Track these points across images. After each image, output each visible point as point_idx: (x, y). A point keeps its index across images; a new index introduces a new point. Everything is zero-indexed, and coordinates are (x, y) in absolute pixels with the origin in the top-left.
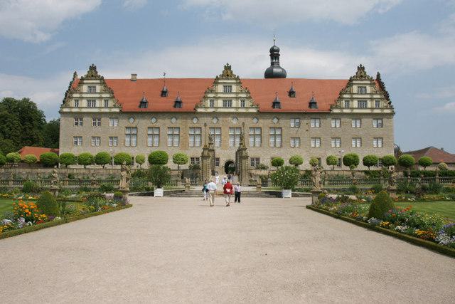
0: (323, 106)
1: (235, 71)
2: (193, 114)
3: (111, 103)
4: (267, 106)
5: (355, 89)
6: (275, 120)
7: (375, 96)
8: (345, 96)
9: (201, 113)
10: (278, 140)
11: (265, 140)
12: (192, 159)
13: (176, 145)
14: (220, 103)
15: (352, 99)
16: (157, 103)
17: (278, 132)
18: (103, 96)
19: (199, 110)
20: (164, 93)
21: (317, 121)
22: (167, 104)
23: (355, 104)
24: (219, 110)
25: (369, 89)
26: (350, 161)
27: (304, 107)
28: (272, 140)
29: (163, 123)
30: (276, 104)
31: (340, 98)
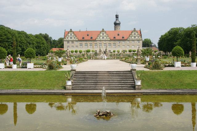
2: (95, 40)
3: (76, 38)
4: (112, 38)
5: (133, 34)
9: (97, 40)
10: (115, 46)
11: (112, 46)
13: (91, 47)
14: (101, 38)
15: (132, 36)
16: (87, 38)
18: (74, 36)
20: (88, 35)
22: (89, 38)
23: (133, 37)
26: (130, 51)
27: (121, 38)
29: (88, 43)
31: (129, 36)
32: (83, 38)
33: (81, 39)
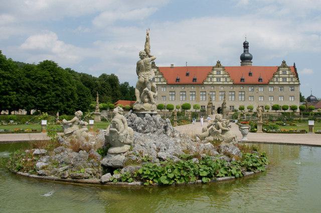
0: (265, 81)
1: (223, 65)
2: (202, 85)
3: (162, 80)
5: (281, 72)
6: (242, 88)
7: (291, 76)
8: (276, 76)
10: (243, 97)
12: (202, 106)
13: (194, 100)
14: (215, 80)
15: (279, 77)
17: (243, 93)
19: (205, 83)
20: (187, 74)
21: (262, 88)
22: (189, 80)
23: (281, 80)
24: (214, 83)
25: (288, 72)
26: (275, 108)
28: (240, 97)
29: (188, 89)
30: (242, 80)
31: (274, 77)
32: (178, 80)
33: (174, 81)
